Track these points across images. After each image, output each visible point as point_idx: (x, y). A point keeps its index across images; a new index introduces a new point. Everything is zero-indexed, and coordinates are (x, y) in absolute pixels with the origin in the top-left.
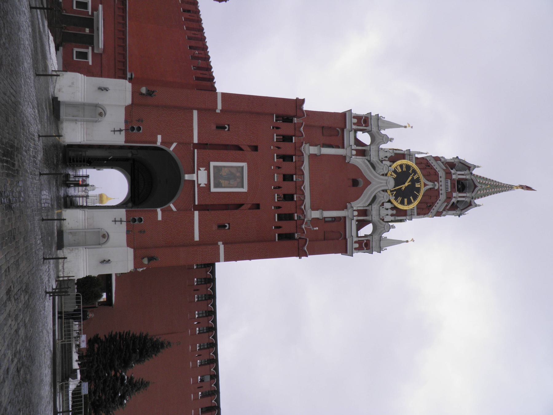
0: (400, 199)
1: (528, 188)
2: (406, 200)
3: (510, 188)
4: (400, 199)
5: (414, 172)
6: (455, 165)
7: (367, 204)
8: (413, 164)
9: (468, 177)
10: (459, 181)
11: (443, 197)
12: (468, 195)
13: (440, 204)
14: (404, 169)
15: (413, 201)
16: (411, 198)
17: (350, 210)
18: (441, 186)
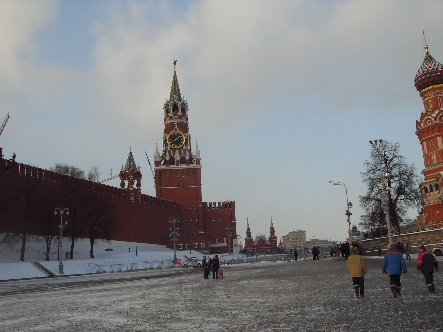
0: (181, 142)
3: (175, 73)
4: (181, 142)
5: (171, 135)
8: (169, 135)
10: (174, 111)
11: (180, 120)
12: (179, 106)
13: (183, 120)
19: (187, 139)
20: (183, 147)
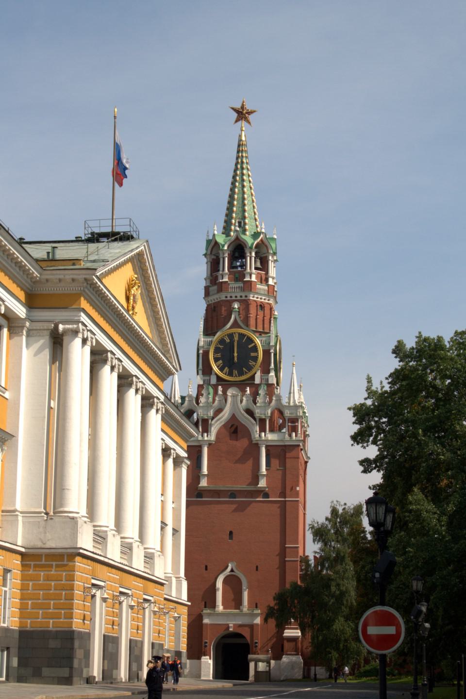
0: (252, 363)
1: (242, 114)
2: (253, 354)
4: (252, 363)
5: (222, 341)
6: (213, 259)
7: (255, 422)
9: (226, 255)
14: (219, 355)
15: (253, 344)
16: (250, 346)
17: (259, 442)
18: (236, 297)
19: (267, 353)
20: (253, 378)
